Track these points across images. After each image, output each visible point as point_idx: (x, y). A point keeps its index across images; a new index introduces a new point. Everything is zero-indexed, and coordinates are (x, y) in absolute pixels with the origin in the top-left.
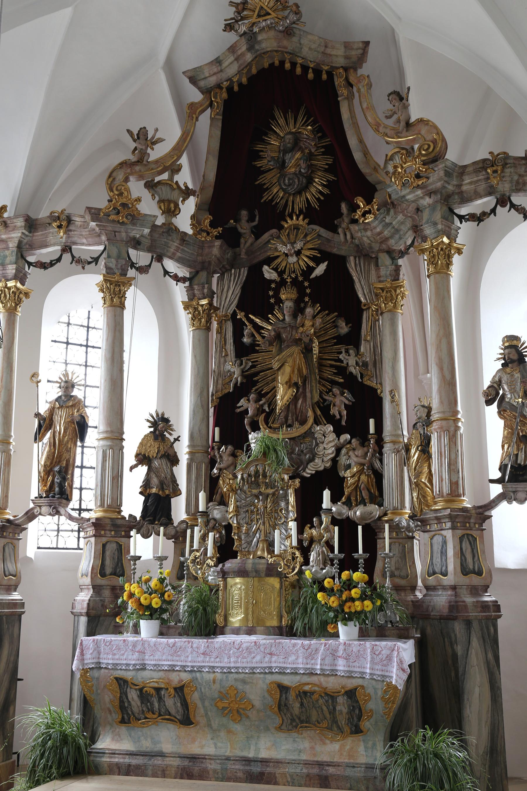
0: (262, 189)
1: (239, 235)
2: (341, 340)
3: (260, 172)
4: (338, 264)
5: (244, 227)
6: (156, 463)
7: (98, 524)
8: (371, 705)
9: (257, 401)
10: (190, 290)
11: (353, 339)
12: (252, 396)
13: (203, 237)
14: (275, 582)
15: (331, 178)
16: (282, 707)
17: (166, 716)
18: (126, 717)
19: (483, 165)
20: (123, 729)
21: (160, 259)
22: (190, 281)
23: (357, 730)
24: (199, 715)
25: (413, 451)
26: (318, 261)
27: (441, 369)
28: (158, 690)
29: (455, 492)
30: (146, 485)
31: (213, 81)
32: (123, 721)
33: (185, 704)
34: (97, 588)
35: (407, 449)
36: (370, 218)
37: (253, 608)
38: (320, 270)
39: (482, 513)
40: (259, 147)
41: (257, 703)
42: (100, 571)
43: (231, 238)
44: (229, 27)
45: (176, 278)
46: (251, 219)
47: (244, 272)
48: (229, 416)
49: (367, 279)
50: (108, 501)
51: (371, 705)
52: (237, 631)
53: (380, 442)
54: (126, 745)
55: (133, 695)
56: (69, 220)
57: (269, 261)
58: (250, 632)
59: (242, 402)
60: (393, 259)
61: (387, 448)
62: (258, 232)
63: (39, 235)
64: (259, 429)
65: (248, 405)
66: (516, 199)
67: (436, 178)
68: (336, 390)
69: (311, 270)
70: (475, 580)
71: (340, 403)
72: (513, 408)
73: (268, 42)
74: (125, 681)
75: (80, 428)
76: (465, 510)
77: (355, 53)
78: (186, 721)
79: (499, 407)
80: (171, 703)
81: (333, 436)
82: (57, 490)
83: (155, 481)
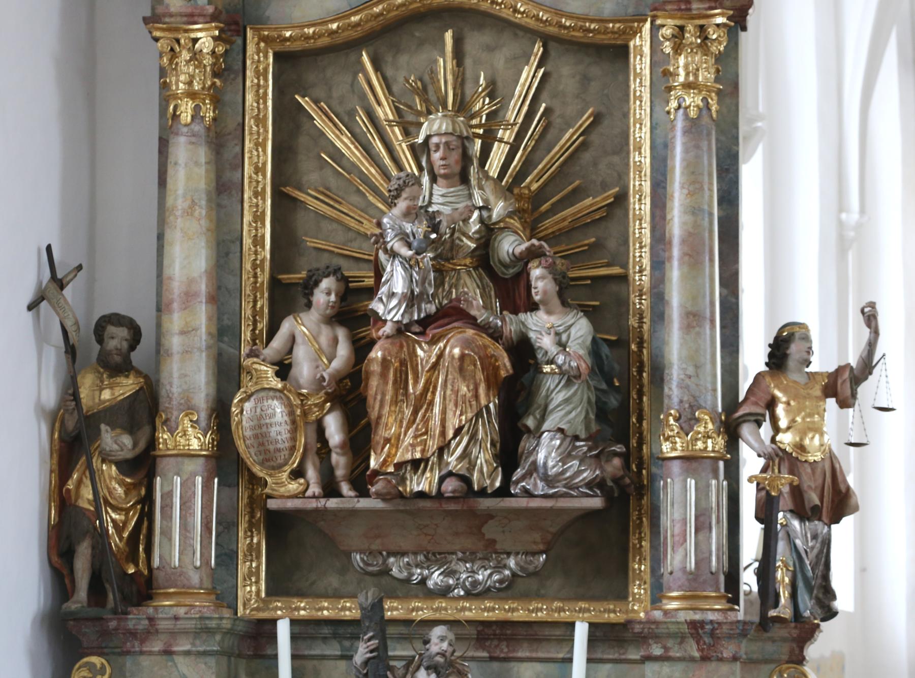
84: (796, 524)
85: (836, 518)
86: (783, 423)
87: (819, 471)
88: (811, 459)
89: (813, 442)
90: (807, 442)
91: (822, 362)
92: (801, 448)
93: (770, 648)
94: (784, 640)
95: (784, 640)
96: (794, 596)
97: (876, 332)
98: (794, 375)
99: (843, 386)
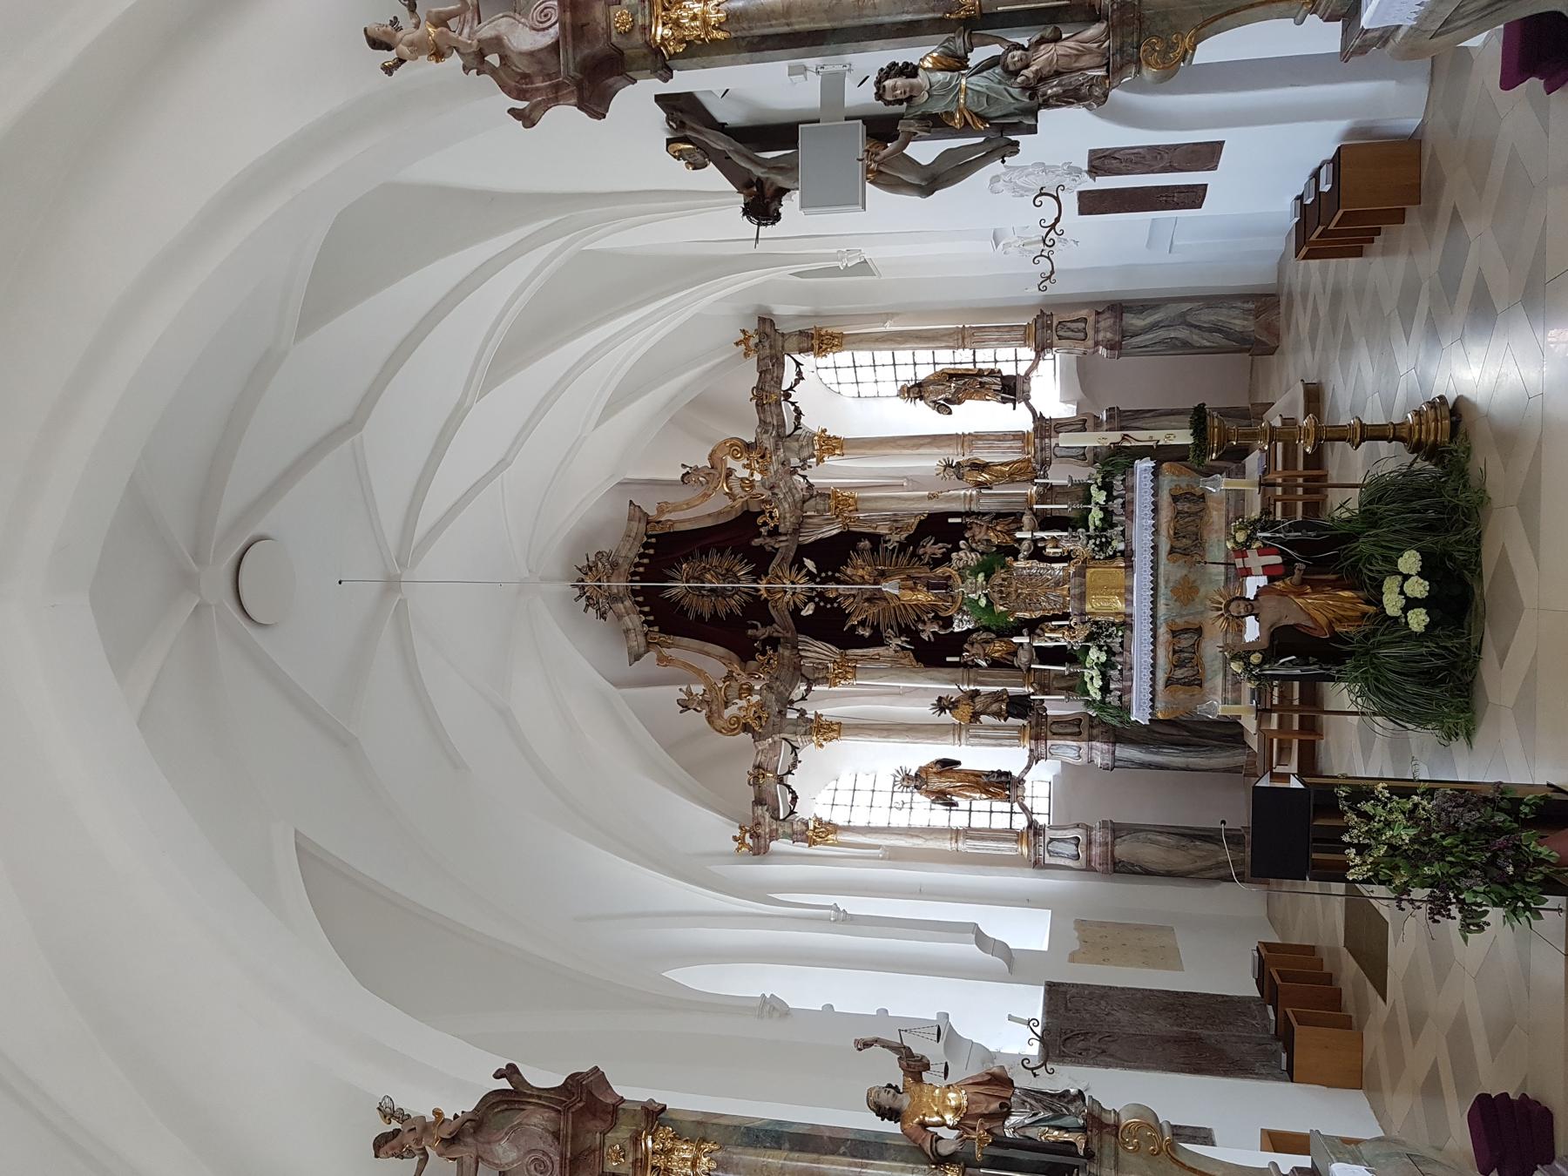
0: (731, 615)
1: (770, 637)
2: (874, 549)
3: (715, 615)
4: (804, 551)
5: (763, 632)
6: (978, 707)
7: (1036, 738)
8: (1183, 485)
9: (924, 623)
10: (817, 681)
11: (876, 539)
12: (920, 627)
13: (774, 663)
14: (1089, 572)
15: (729, 551)
16: (1185, 552)
17: (1196, 647)
18: (1196, 682)
19: (760, 406)
20: (1207, 685)
21: (792, 702)
22: (810, 683)
23: (1203, 497)
24: (1194, 621)
25: (981, 479)
26: (802, 566)
27: (921, 445)
28: (1175, 652)
29: (1019, 436)
30: (997, 715)
31: (641, 639)
32: (1200, 685)
33: (1185, 631)
34: (1091, 738)
35: (979, 485)
36: (776, 513)
37: (1108, 590)
38: (810, 564)
39: (1038, 419)
40: (691, 616)
41: (1184, 572)
42: (1077, 735)
43: (773, 642)
44: (603, 616)
45: (808, 690)
46: (755, 627)
47: (801, 638)
48: (934, 653)
49: (820, 526)
50: (1015, 734)
51: (1183, 485)
52: (1129, 603)
53: (969, 514)
54: (1219, 680)
55: (1179, 673)
56: (758, 767)
57: (796, 611)
58: (1130, 590)
59: (925, 636)
60: (812, 496)
61: (974, 508)
62: (768, 621)
63: (769, 800)
64: (951, 617)
65: (929, 631)
66: (785, 386)
67: (768, 443)
68: (921, 551)
69: (809, 573)
70: (1090, 423)
71: (932, 548)
72: (958, 390)
73: (618, 584)
74: (1168, 679)
75: (947, 765)
76: (1035, 430)
77: (638, 514)
78: (1199, 631)
79: (953, 403)
80: (1185, 642)
81: (962, 554)
82: (1002, 785)
83: (994, 707)
84: (1013, 1120)
85: (1009, 1083)
86: (936, 1119)
87: (975, 1098)
88: (965, 1103)
89: (953, 1098)
90: (953, 1103)
91: (898, 1078)
92: (957, 1109)
93: (1107, 1151)
94: (1100, 1140)
95: (1100, 1140)
96: (1067, 1130)
97: (876, 1041)
98: (905, 1102)
99: (915, 1067)
